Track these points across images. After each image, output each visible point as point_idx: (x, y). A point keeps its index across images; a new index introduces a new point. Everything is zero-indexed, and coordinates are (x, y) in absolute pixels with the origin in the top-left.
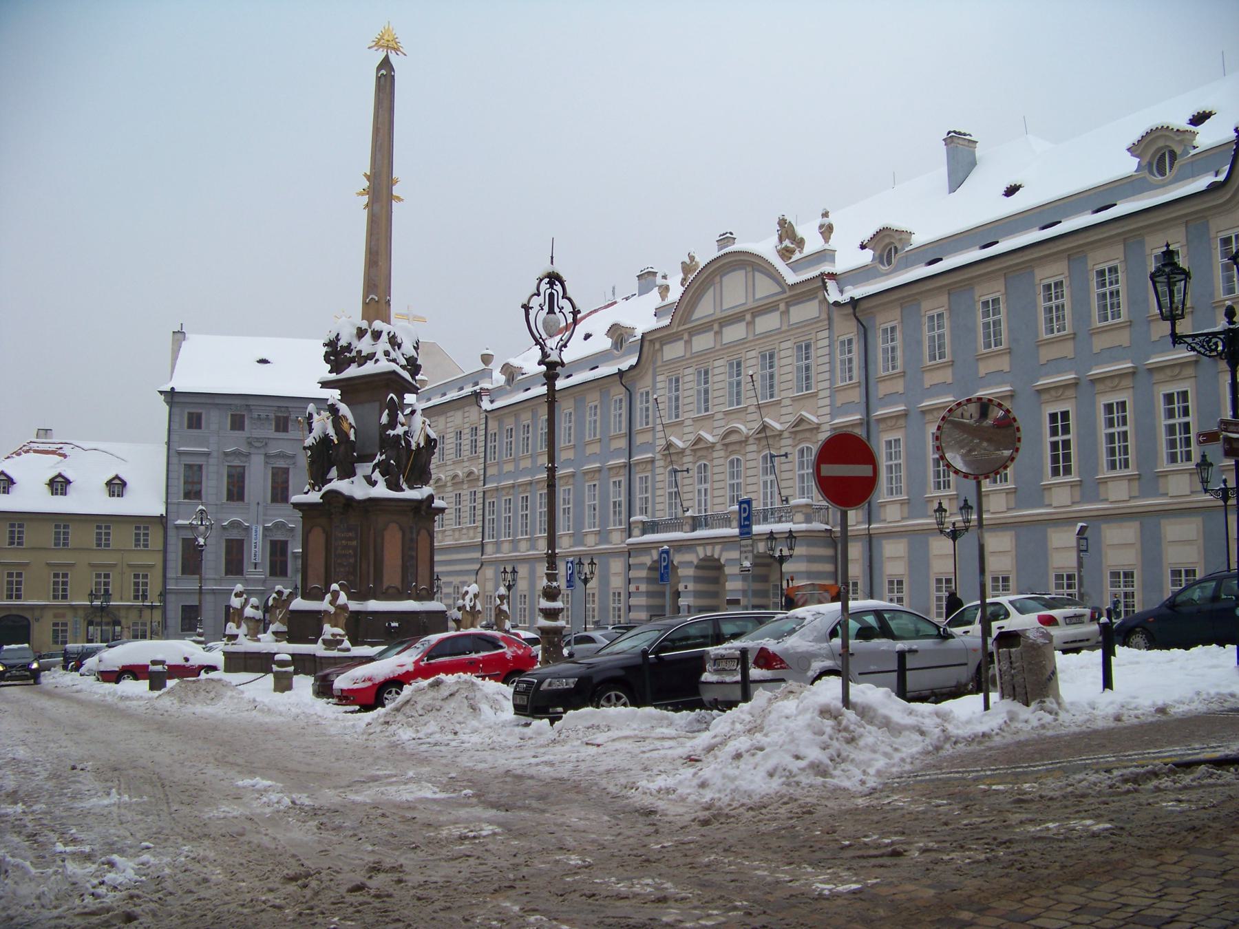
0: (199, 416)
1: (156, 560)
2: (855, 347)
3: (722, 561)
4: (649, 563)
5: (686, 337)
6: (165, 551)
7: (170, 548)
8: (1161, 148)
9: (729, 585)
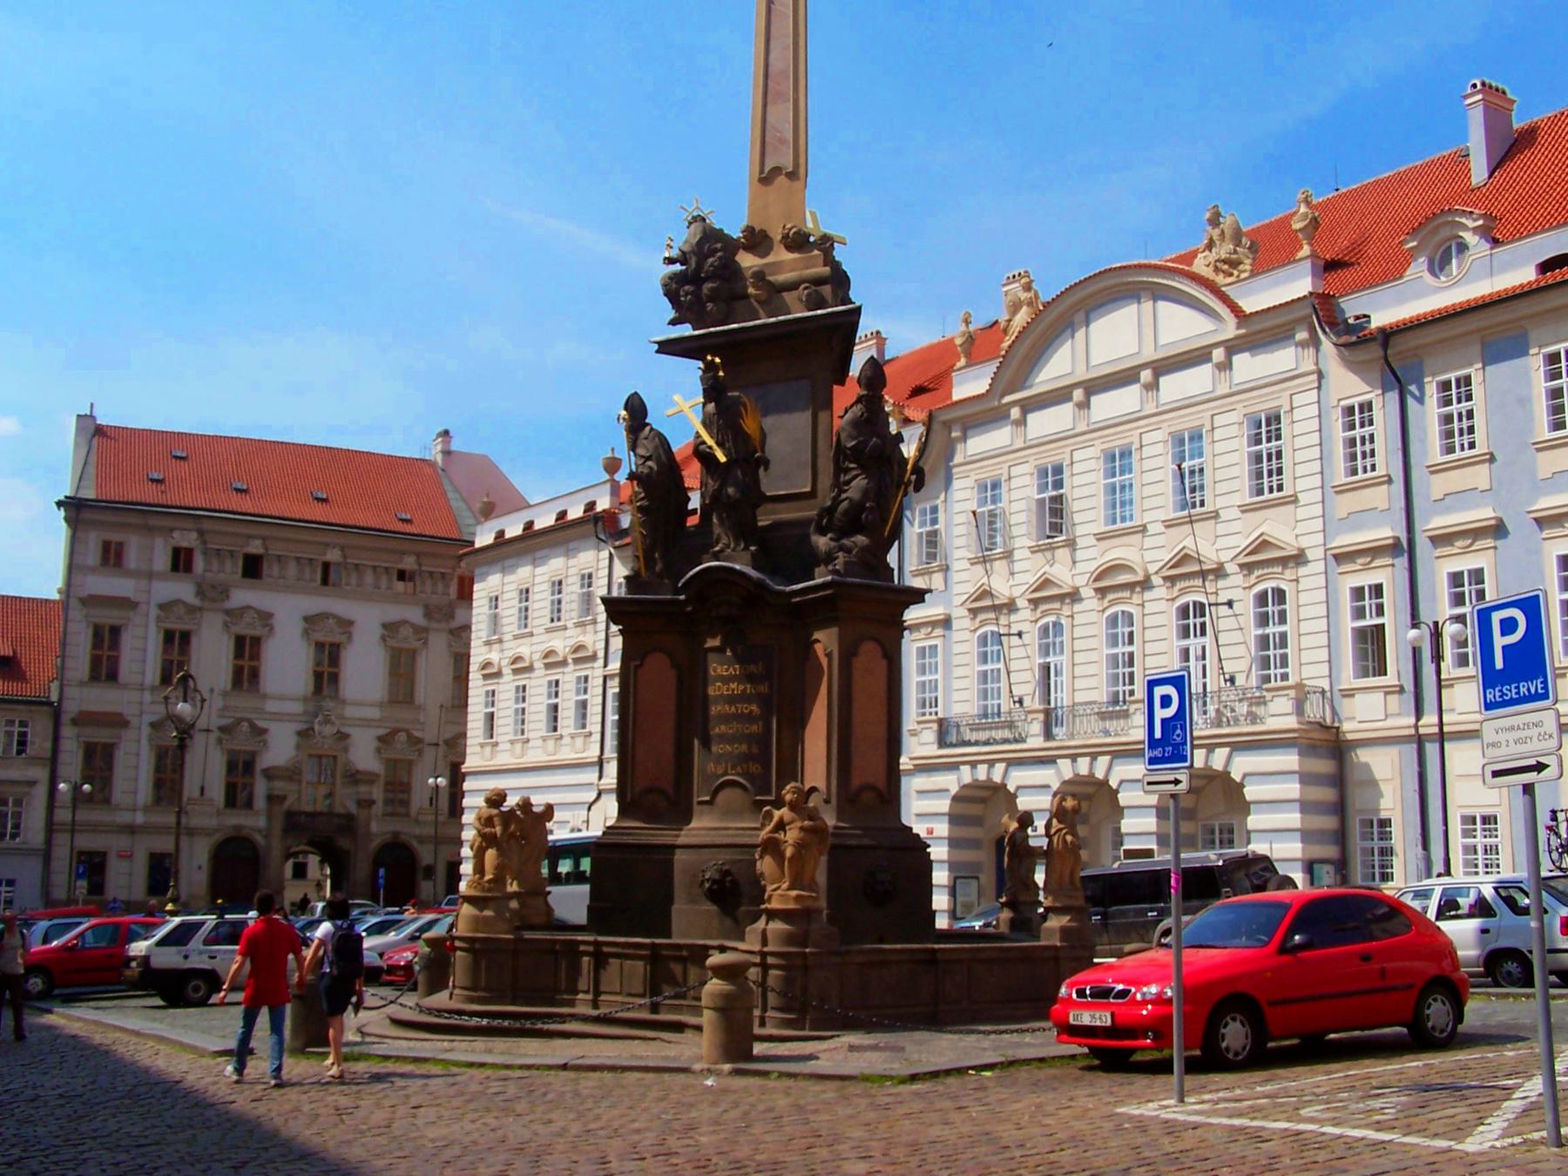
0: (120, 546)
1: (41, 774)
2: (1377, 414)
3: (1113, 783)
4: (954, 789)
5: (1015, 413)
6: (54, 761)
7: (64, 757)
8: (1449, 239)
9: (1128, 824)
